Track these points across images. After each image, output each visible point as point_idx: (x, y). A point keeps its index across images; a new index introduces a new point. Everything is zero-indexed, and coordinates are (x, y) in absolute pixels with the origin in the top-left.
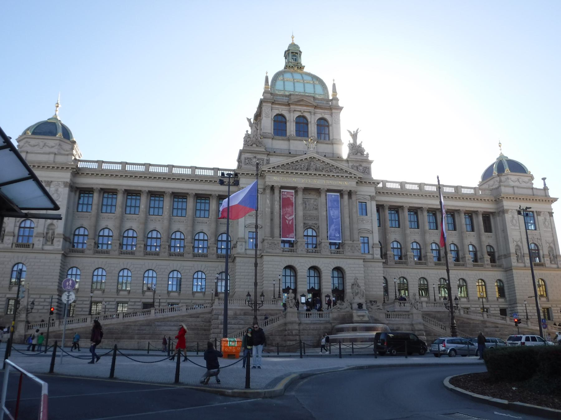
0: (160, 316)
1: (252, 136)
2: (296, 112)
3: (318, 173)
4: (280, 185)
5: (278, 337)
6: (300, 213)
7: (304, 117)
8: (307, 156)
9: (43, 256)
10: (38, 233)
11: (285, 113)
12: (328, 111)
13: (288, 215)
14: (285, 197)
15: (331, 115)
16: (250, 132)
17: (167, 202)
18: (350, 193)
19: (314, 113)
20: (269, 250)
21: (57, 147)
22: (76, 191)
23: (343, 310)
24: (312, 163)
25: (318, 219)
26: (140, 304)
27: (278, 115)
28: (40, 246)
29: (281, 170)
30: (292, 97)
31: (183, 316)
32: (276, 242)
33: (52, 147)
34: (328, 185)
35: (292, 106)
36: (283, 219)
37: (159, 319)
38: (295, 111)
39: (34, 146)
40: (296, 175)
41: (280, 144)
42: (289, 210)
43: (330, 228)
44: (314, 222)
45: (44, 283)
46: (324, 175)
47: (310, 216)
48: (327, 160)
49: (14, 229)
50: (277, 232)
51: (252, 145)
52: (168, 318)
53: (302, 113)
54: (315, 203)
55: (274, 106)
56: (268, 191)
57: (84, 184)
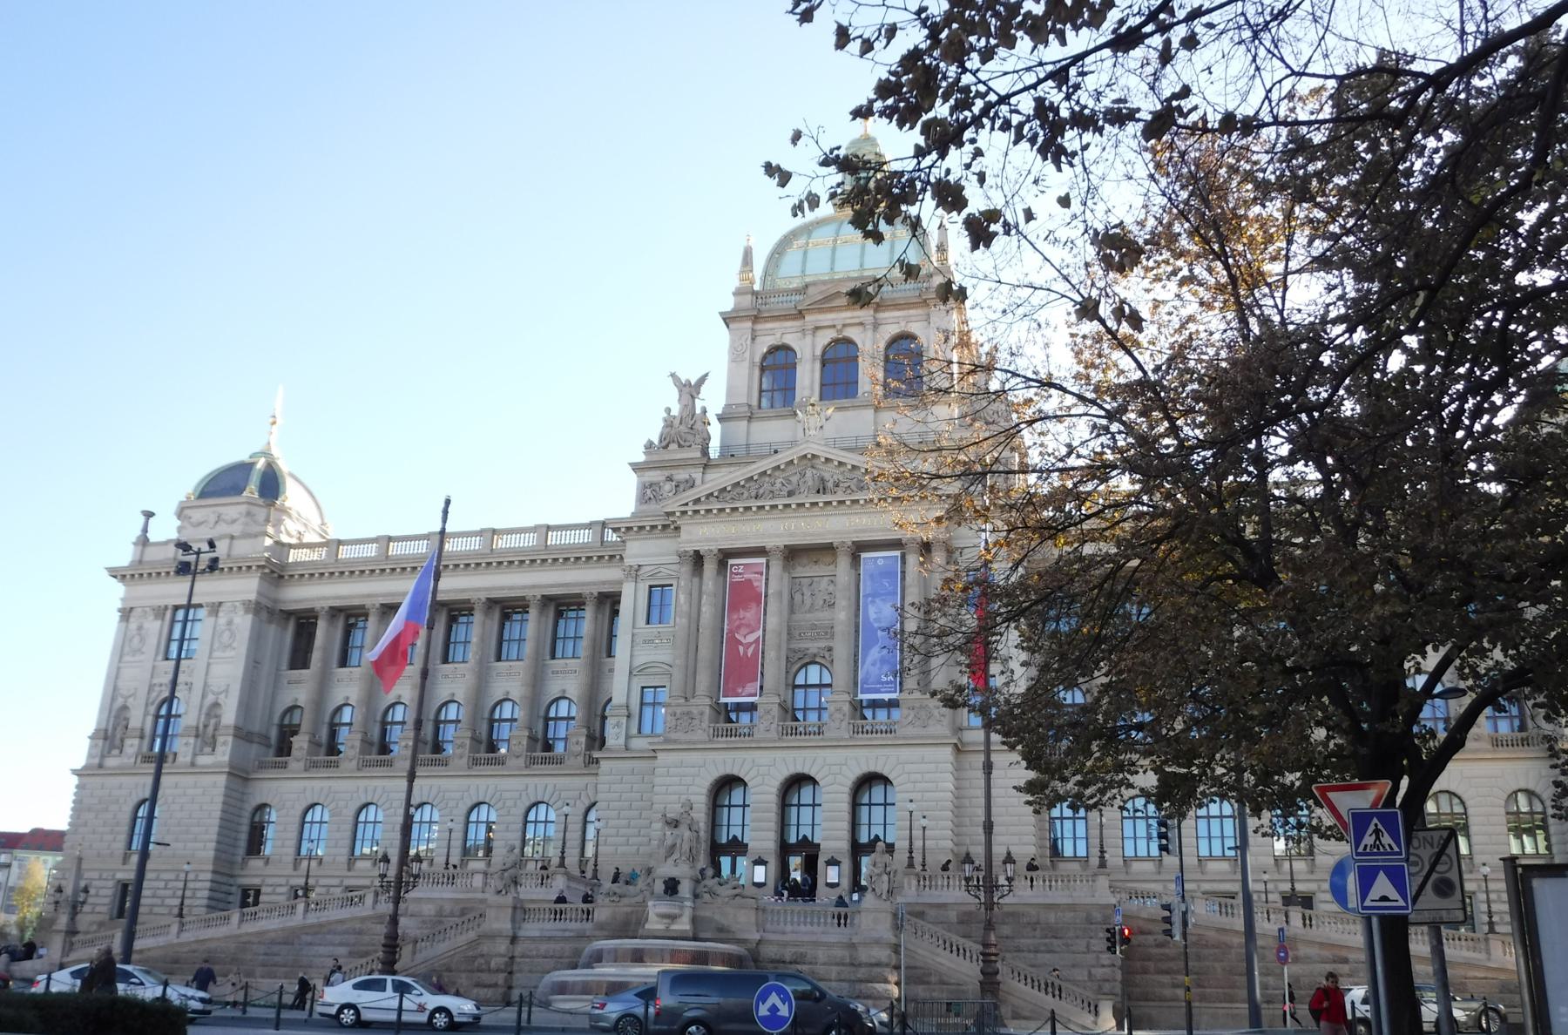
0: (313, 918)
1: (677, 422)
2: (820, 333)
3: (821, 499)
4: (714, 547)
5: (463, 975)
6: (773, 621)
7: (849, 342)
8: (793, 454)
9: (190, 779)
10: (187, 728)
11: (789, 340)
12: (920, 311)
13: (744, 631)
14: (737, 579)
15: (928, 320)
16: (675, 411)
17: (531, 627)
18: (926, 548)
19: (876, 325)
20: (673, 736)
21: (243, 520)
22: (288, 619)
23: (625, 901)
24: (809, 473)
25: (832, 637)
26: (284, 890)
27: (774, 350)
28: (188, 759)
29: (716, 506)
30: (811, 290)
31: (363, 919)
32: (695, 711)
33: (234, 521)
34: (856, 531)
35: (808, 318)
36: (727, 642)
37: (312, 926)
38: (817, 328)
39: (200, 524)
40: (762, 514)
41: (771, 431)
42: (748, 615)
43: (865, 656)
44: (823, 644)
45: (190, 845)
46: (841, 502)
47: (814, 627)
48: (851, 459)
49: (144, 722)
50: (703, 681)
51: (666, 447)
52: (329, 923)
53: (840, 331)
54: (831, 588)
55: (759, 327)
56: (686, 569)
57: (296, 601)
